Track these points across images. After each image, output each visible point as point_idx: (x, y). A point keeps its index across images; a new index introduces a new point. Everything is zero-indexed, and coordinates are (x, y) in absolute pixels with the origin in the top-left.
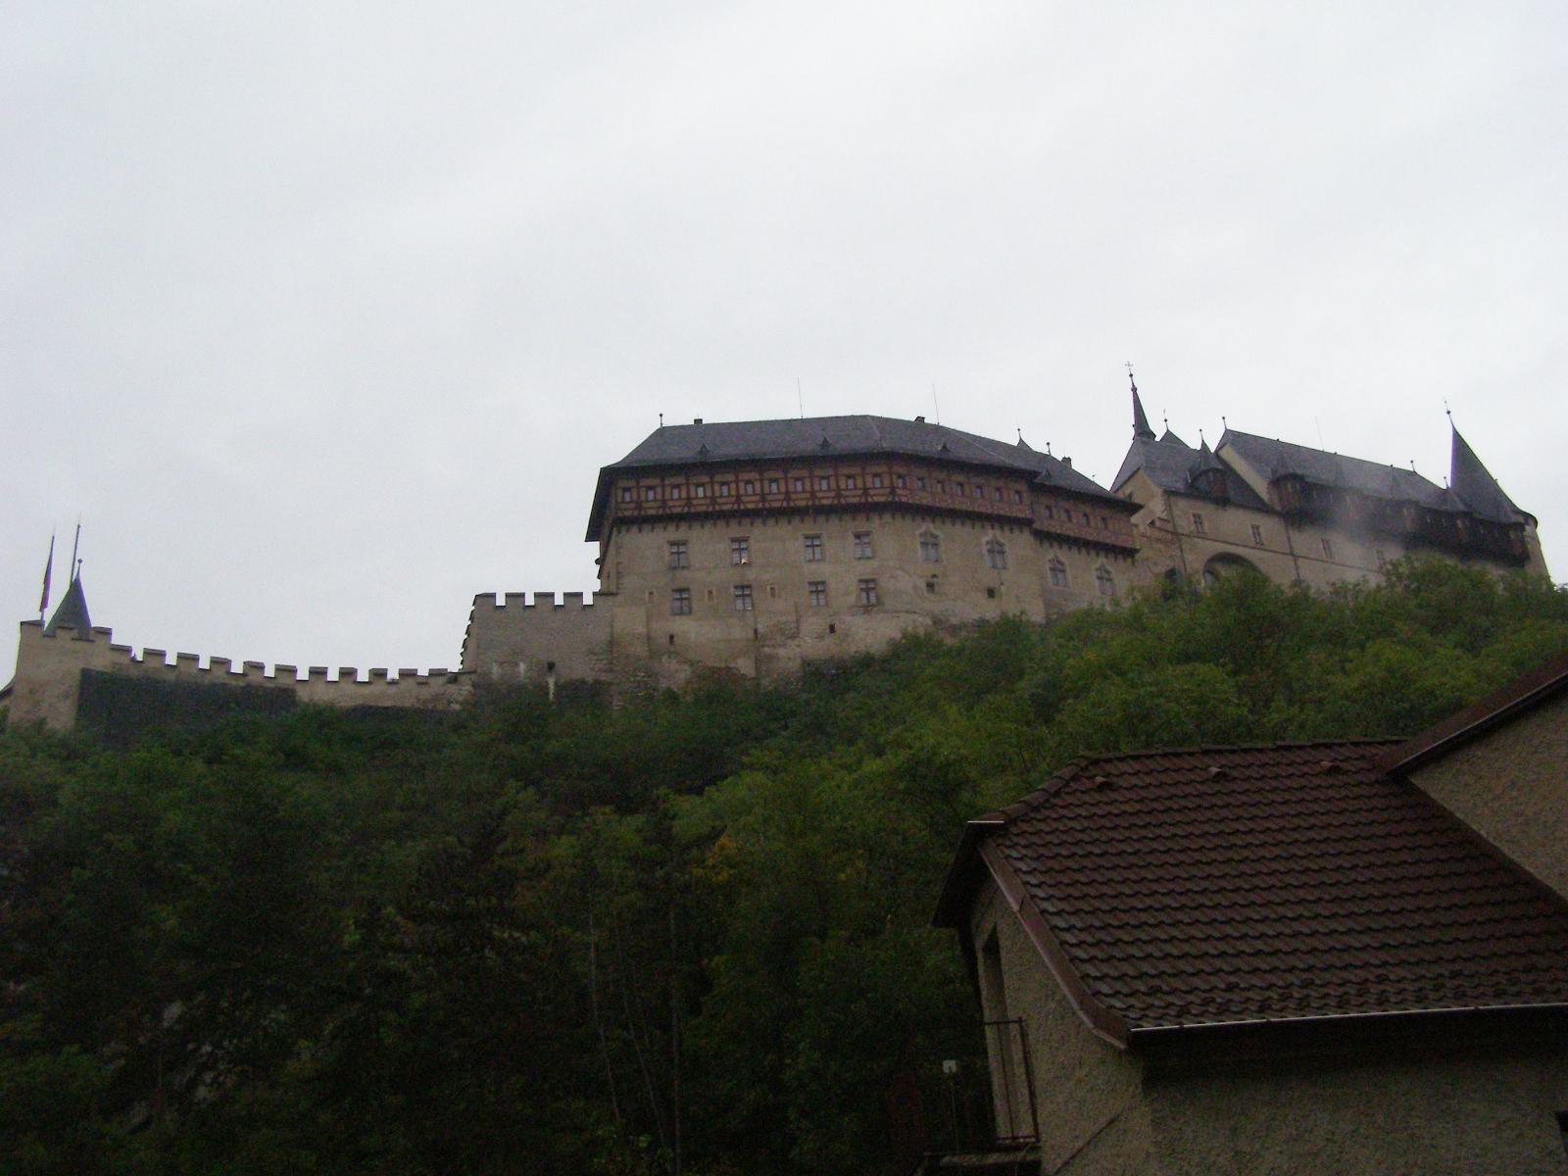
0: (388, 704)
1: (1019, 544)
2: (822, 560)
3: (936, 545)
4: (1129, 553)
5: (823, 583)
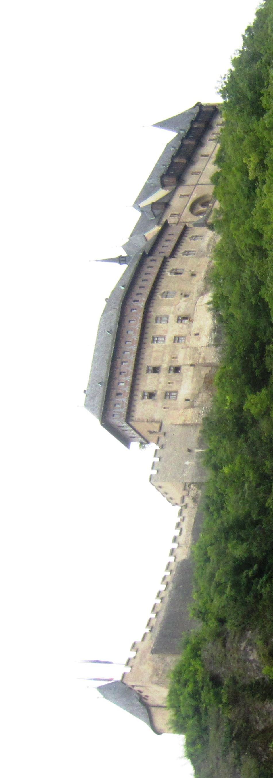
0: (193, 520)
1: (174, 263)
2: (164, 337)
3: (168, 292)
4: (185, 229)
5: (175, 337)
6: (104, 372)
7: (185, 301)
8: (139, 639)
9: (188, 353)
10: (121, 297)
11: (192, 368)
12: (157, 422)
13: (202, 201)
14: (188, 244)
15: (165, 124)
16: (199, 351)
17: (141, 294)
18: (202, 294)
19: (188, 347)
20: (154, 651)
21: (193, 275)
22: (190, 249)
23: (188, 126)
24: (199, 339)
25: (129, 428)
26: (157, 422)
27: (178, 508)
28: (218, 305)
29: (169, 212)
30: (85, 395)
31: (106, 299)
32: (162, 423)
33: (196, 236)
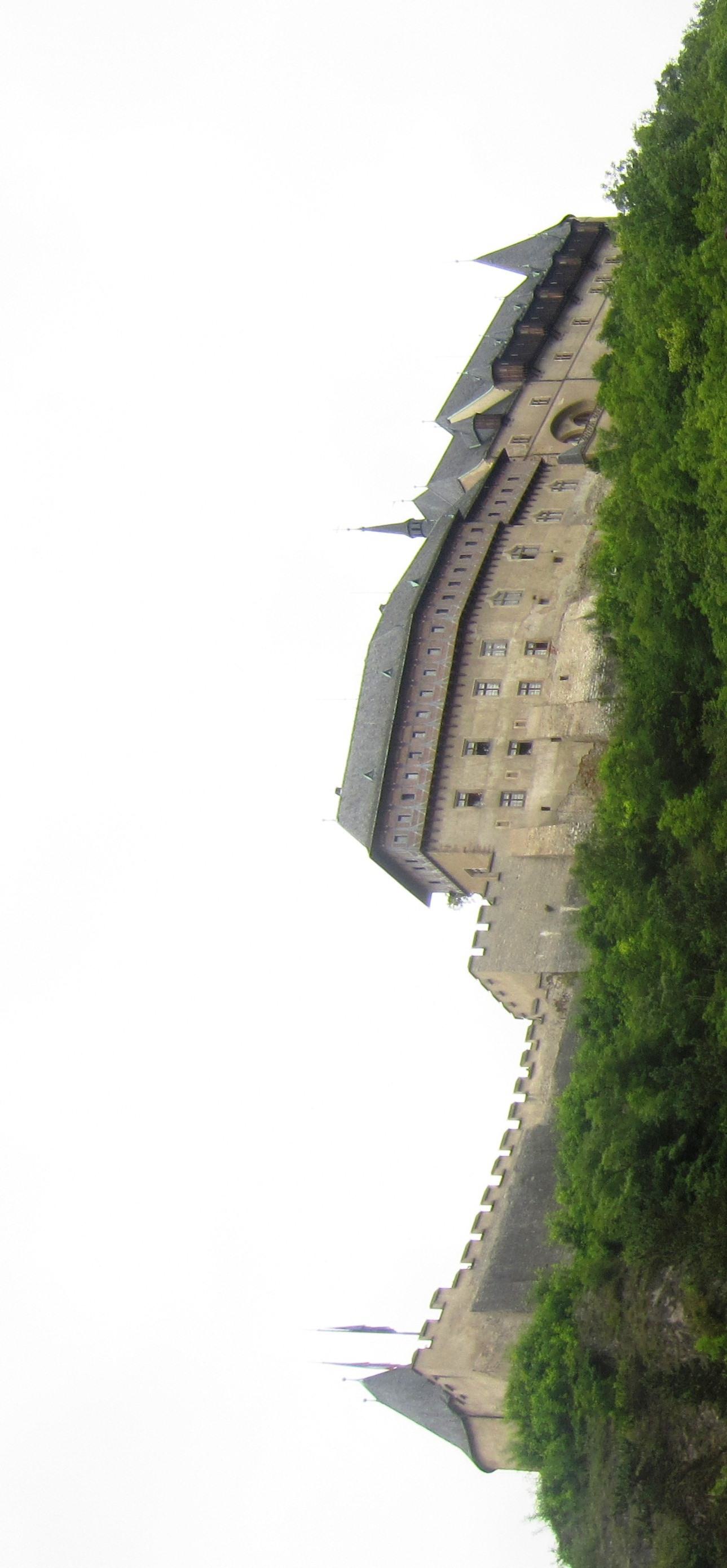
0: (557, 1047)
1: (518, 536)
3: (506, 594)
4: (542, 468)
5: (521, 684)
6: (378, 751)
7: (541, 612)
8: (448, 1283)
9: (547, 717)
10: (410, 604)
11: (555, 744)
12: (484, 852)
13: (576, 413)
14: (547, 498)
15: (499, 258)
16: (569, 712)
17: (452, 597)
18: (576, 598)
19: (547, 704)
20: (477, 1308)
21: (557, 560)
22: (553, 509)
23: (549, 262)
24: (569, 688)
25: (428, 864)
26: (484, 852)
27: (527, 1023)
28: (609, 619)
29: (510, 433)
30: (338, 797)
31: (382, 607)
32: (494, 854)
33: (564, 483)
